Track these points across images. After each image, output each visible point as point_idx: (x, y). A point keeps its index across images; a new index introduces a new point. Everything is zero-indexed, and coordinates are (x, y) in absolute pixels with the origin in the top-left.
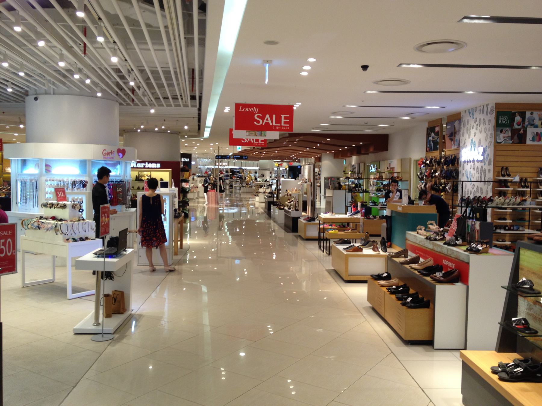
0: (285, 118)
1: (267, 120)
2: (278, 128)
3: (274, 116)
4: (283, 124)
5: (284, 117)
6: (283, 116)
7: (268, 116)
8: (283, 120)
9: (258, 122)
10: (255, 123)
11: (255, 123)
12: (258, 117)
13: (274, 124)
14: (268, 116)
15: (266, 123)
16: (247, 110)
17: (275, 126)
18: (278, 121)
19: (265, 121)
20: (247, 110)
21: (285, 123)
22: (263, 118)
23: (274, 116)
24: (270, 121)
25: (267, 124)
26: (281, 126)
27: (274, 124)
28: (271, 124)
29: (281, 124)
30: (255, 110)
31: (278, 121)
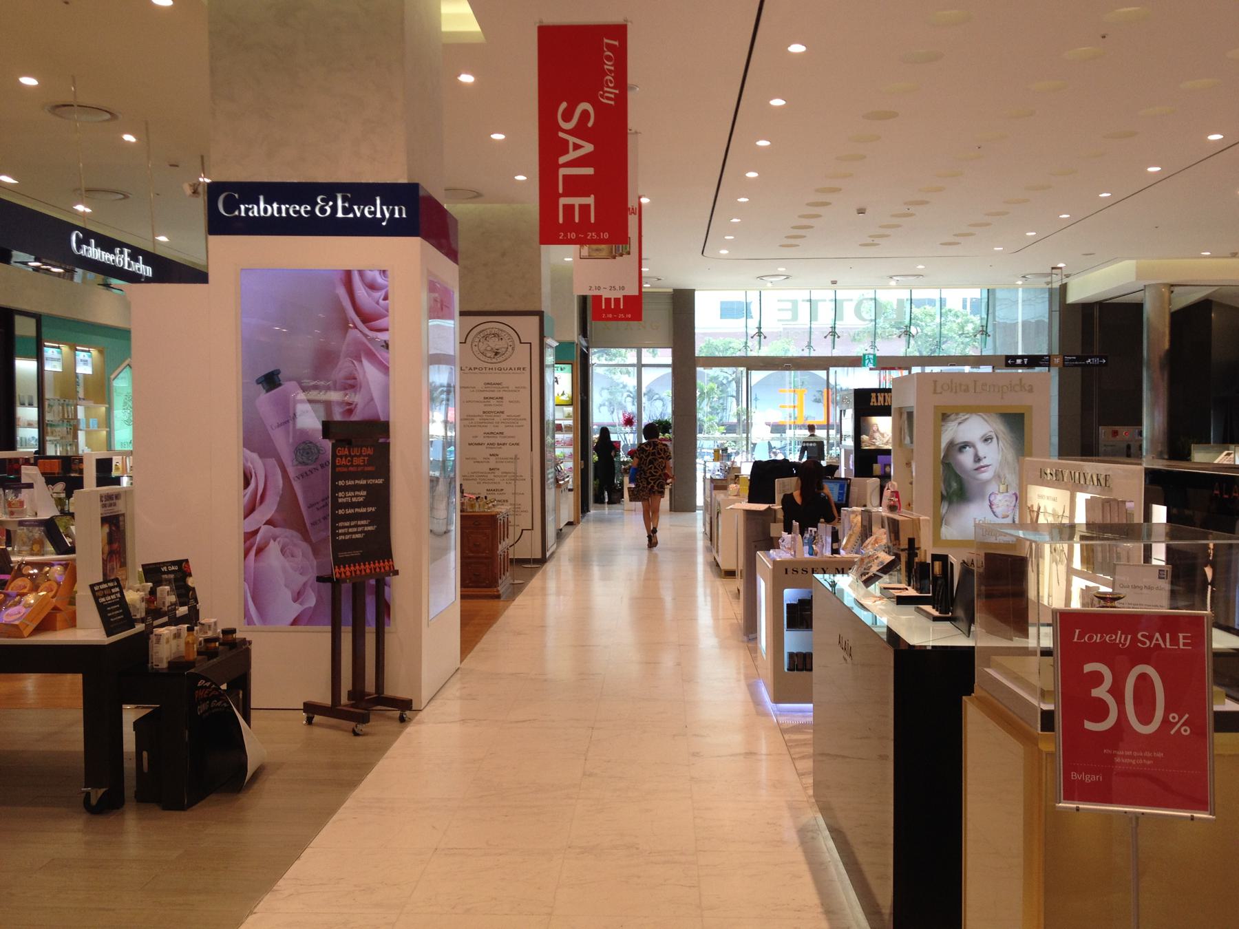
0: (584, 209)
1: (577, 147)
3: (589, 171)
4: (563, 201)
5: (589, 206)
7: (588, 148)
8: (577, 201)
10: (564, 105)
11: (564, 105)
12: (585, 114)
13: (563, 171)
14: (588, 148)
15: (567, 142)
16: (609, 66)
18: (576, 186)
19: (572, 140)
20: (609, 66)
21: (569, 209)
23: (589, 171)
24: (572, 155)
25: (563, 148)
27: (563, 171)
28: (562, 160)
29: (565, 194)
30: (608, 94)
31: (576, 186)
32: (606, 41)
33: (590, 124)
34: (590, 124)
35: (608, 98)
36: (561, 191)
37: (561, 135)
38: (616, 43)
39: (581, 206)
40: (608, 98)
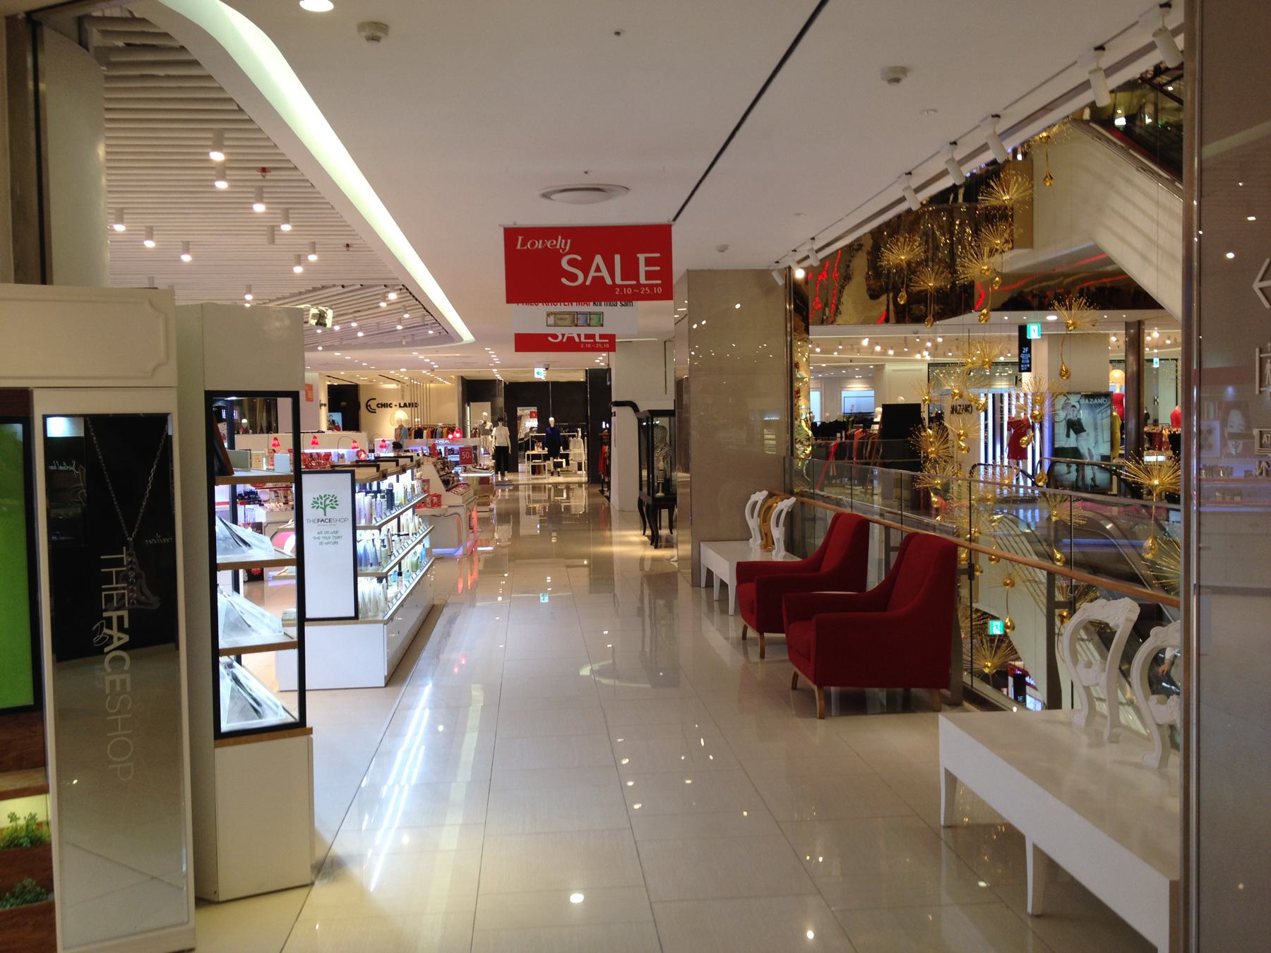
0: (649, 262)
1: (598, 269)
2: (629, 291)
3: (617, 258)
4: (643, 280)
6: (642, 257)
7: (598, 259)
8: (643, 269)
9: (573, 277)
10: (564, 281)
11: (564, 281)
12: (570, 262)
13: (618, 281)
14: (598, 259)
16: (539, 245)
17: (621, 287)
19: (592, 273)
20: (539, 245)
21: (649, 275)
22: (585, 267)
23: (617, 258)
24: (605, 273)
26: (639, 285)
27: (618, 281)
28: (609, 282)
29: (638, 280)
30: (560, 243)
31: (630, 270)
33: (579, 258)
34: (579, 258)
37: (588, 283)
39: (647, 265)
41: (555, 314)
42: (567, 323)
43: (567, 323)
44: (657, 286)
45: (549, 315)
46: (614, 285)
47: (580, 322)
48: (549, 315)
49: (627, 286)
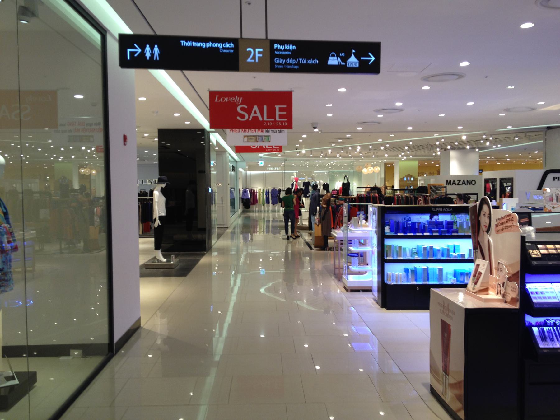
0: (281, 110)
1: (255, 113)
3: (265, 107)
4: (277, 119)
6: (277, 107)
7: (256, 108)
8: (278, 113)
9: (243, 117)
10: (238, 118)
11: (238, 118)
12: (242, 109)
14: (256, 108)
16: (226, 100)
17: (267, 122)
18: (271, 114)
19: (252, 115)
20: (226, 100)
21: (281, 116)
22: (249, 111)
24: (259, 115)
26: (275, 121)
27: (265, 119)
28: (261, 119)
29: (275, 118)
30: (237, 99)
32: (216, 101)
33: (246, 107)
34: (246, 107)
35: (239, 100)
36: (273, 120)
37: (250, 119)
38: (217, 96)
40: (239, 100)
41: (248, 136)
42: (253, 140)
43: (253, 140)
44: (284, 121)
45: (245, 137)
46: (263, 121)
47: (259, 140)
48: (245, 137)
49: (270, 121)
